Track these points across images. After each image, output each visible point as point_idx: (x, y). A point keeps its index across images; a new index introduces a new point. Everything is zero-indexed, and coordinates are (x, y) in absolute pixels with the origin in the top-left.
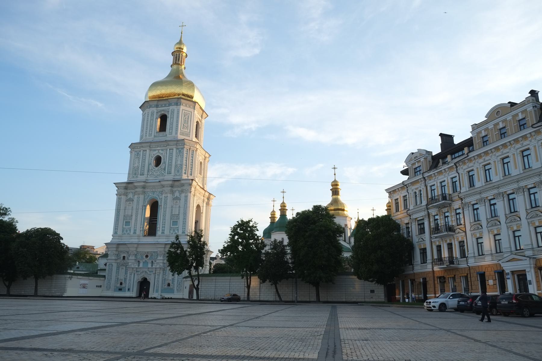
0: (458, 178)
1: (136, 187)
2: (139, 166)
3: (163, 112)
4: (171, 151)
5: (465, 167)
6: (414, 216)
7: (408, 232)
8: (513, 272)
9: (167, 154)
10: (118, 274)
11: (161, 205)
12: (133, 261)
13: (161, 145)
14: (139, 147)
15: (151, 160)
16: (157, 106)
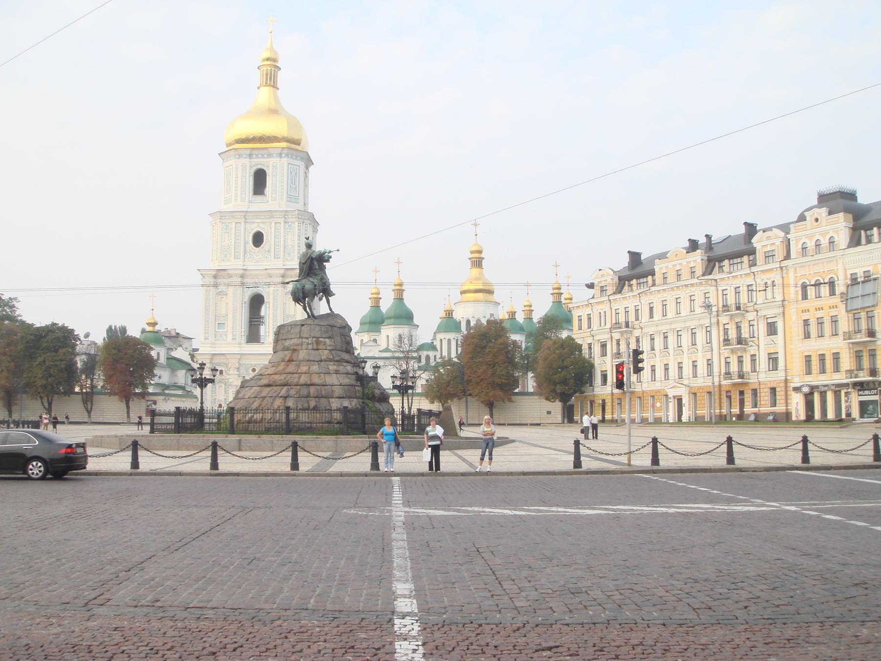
0: (640, 306)
1: (230, 276)
2: (231, 245)
3: (260, 167)
4: (278, 225)
5: (647, 299)
6: (597, 338)
7: (590, 353)
8: (674, 397)
9: (271, 229)
10: (215, 393)
11: (269, 302)
12: (237, 376)
13: (261, 216)
14: (228, 217)
15: (248, 236)
16: (250, 156)
